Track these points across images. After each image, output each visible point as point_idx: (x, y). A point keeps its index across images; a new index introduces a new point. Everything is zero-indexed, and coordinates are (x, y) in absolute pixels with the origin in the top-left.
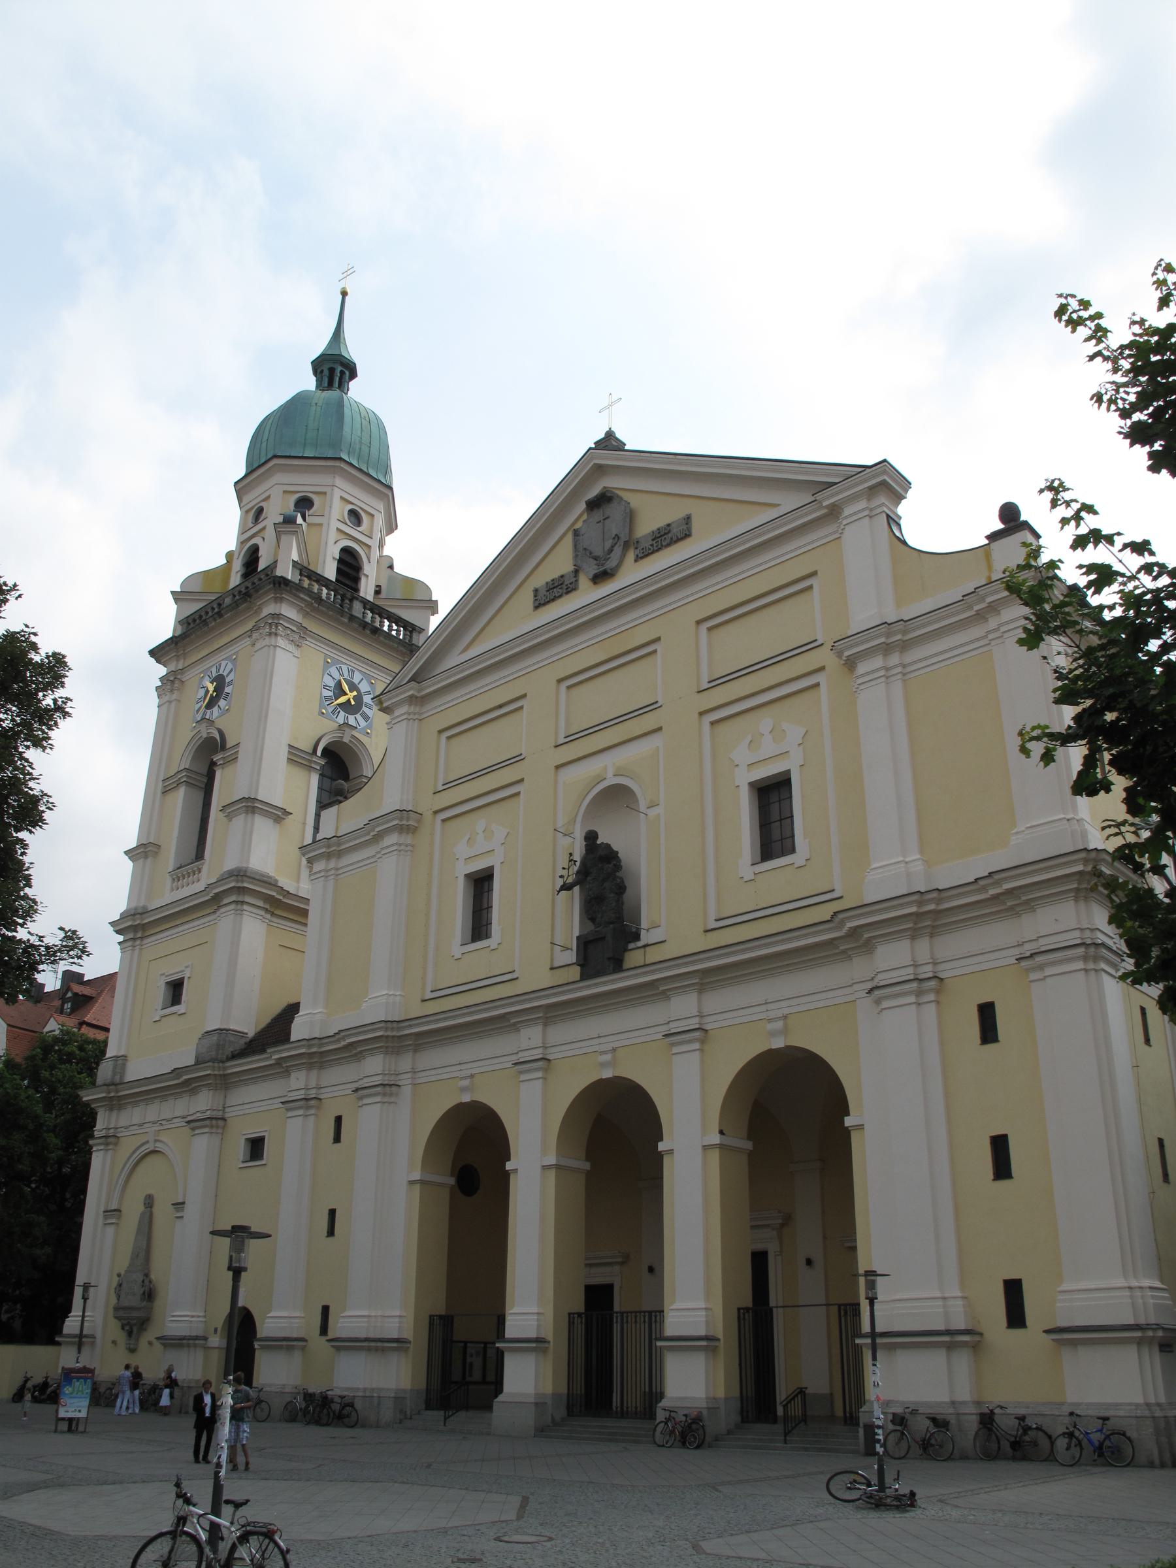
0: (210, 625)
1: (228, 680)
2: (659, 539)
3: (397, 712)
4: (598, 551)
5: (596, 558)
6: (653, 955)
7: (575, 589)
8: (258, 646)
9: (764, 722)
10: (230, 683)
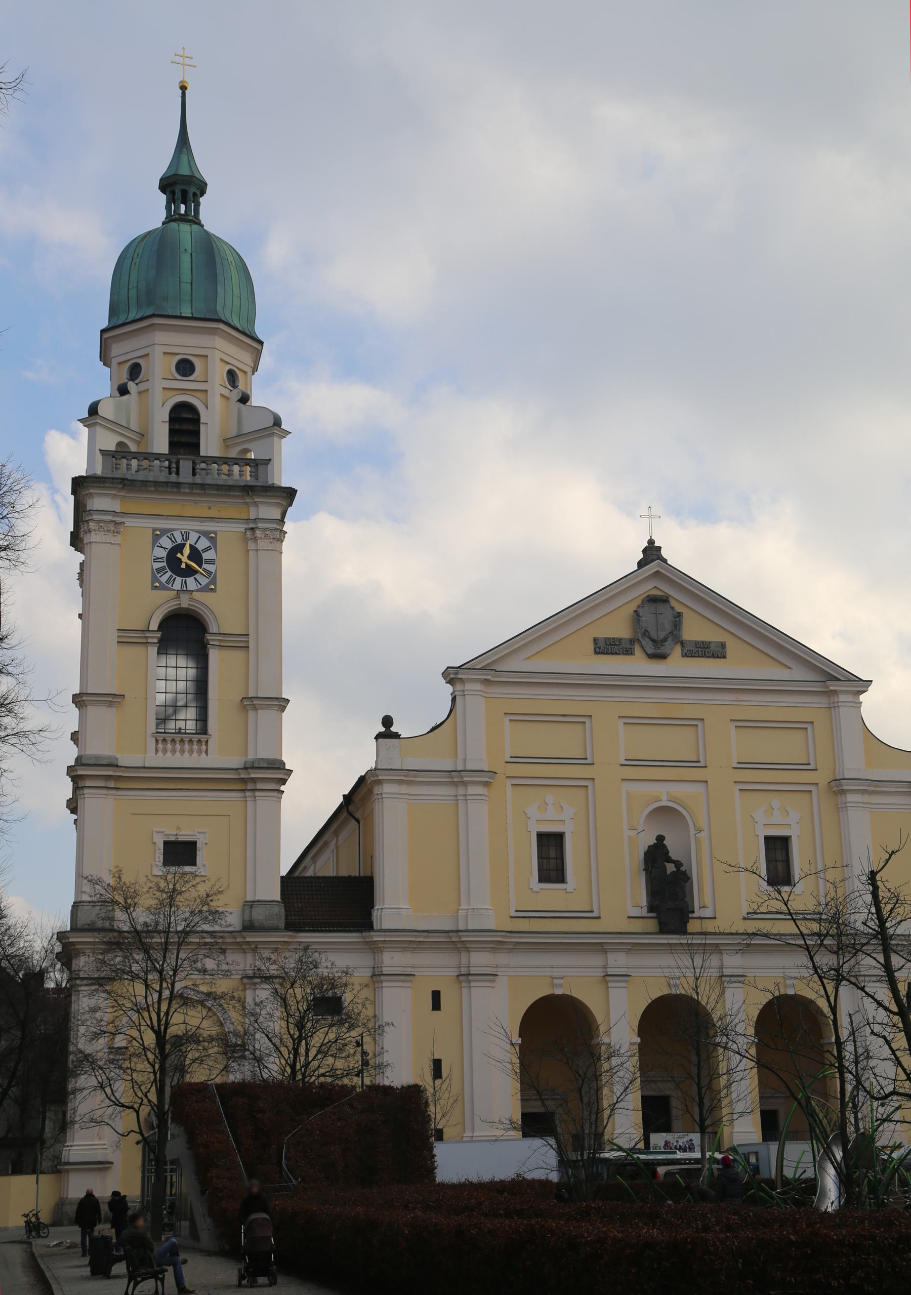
0: (182, 490)
1: (205, 556)
2: (704, 650)
3: (468, 686)
4: (654, 636)
5: (653, 641)
6: (709, 926)
7: (631, 654)
8: (262, 544)
9: (776, 801)
10: (211, 562)
